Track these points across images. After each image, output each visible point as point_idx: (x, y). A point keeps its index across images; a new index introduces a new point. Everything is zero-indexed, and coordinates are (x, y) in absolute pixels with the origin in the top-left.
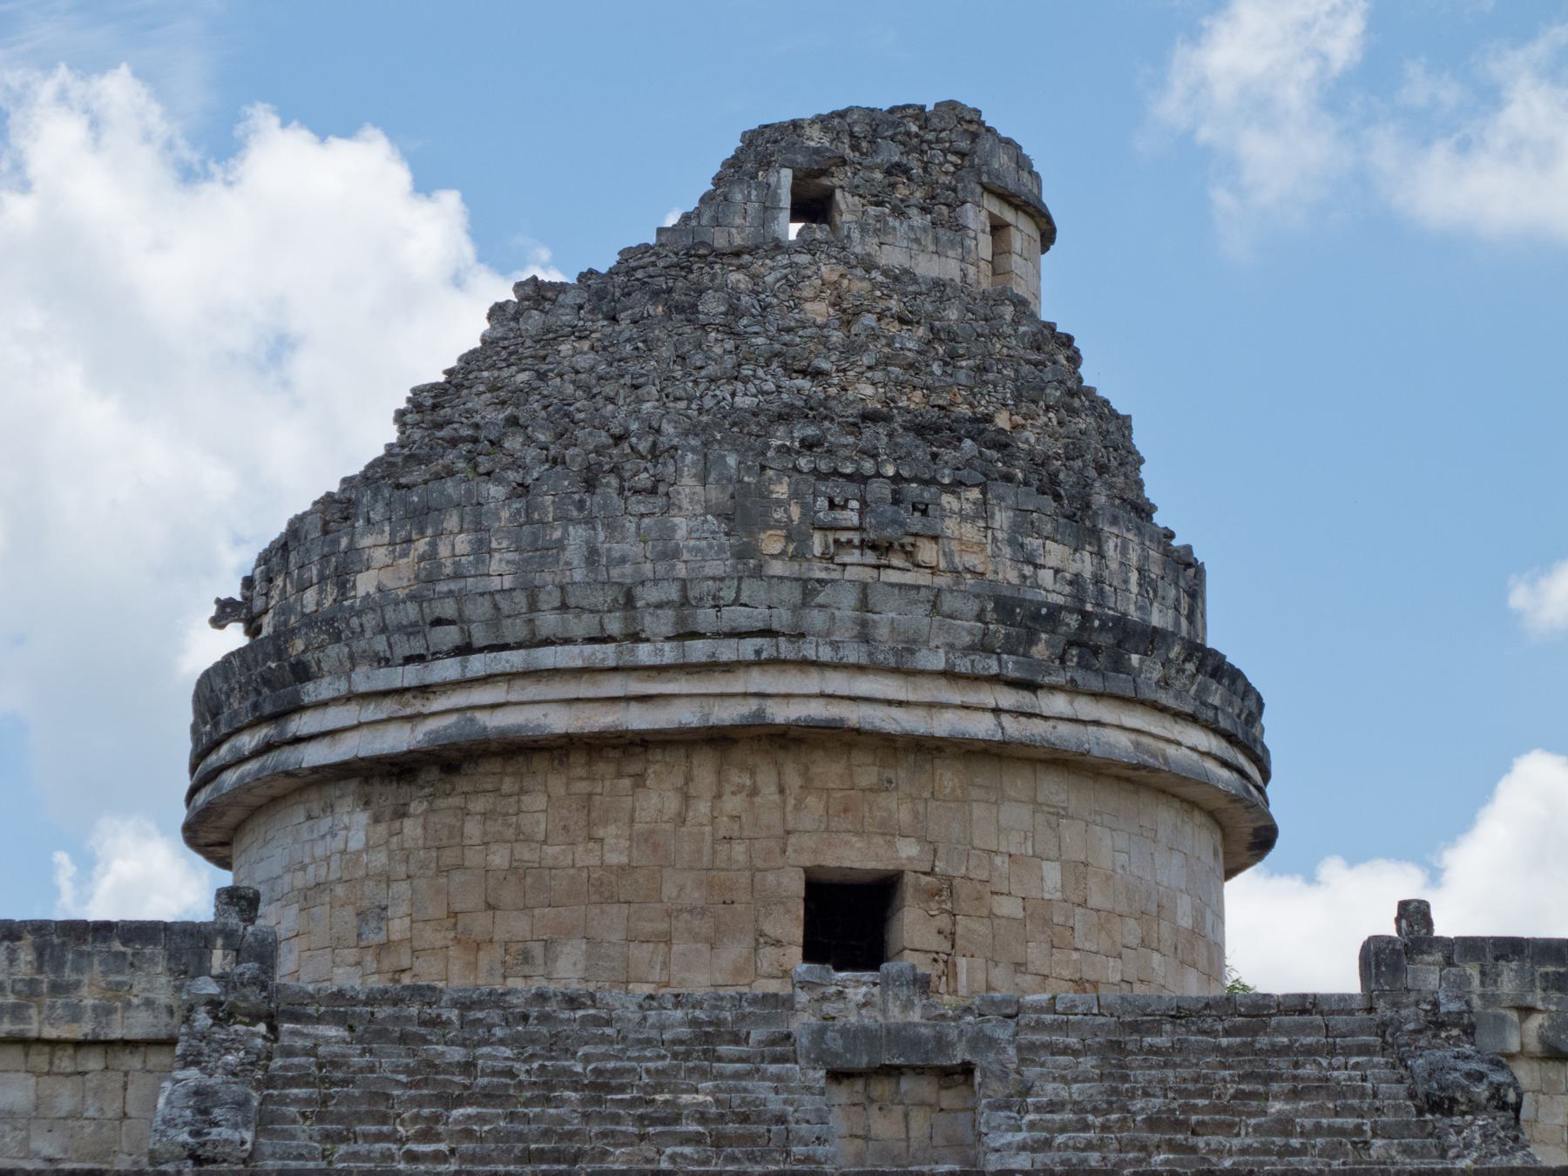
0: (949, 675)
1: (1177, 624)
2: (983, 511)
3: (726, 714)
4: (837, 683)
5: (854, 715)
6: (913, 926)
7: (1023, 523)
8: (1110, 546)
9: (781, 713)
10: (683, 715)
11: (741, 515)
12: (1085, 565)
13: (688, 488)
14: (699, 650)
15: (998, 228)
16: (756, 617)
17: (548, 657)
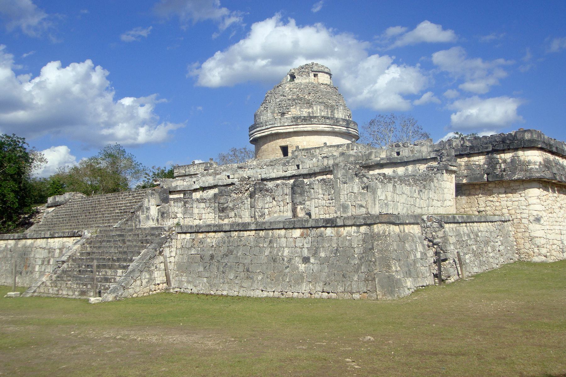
0: (288, 126)
1: (328, 114)
2: (296, 108)
3: (269, 133)
4: (278, 128)
5: (279, 131)
6: (290, 151)
7: (301, 108)
8: (315, 108)
9: (273, 132)
10: (266, 133)
11: (273, 113)
12: (310, 110)
13: (269, 111)
14: (267, 127)
15: (315, 75)
16: (270, 123)
17: (258, 129)
